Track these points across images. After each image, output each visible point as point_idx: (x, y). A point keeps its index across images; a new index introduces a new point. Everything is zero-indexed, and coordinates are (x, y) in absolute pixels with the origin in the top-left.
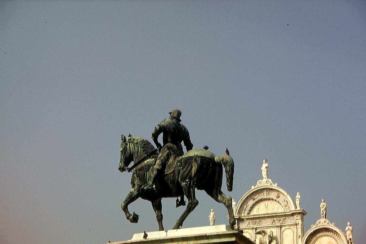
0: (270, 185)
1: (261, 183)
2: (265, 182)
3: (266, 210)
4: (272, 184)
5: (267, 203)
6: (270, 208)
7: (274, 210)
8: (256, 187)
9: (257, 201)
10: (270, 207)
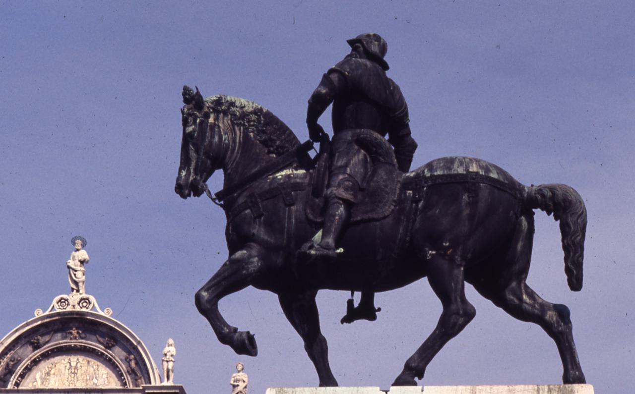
0: (91, 310)
1: (64, 302)
2: (76, 303)
3: (70, 379)
4: (98, 309)
5: (75, 360)
6: (82, 375)
7: (95, 381)
8: (47, 313)
9: (47, 352)
10: (83, 372)
